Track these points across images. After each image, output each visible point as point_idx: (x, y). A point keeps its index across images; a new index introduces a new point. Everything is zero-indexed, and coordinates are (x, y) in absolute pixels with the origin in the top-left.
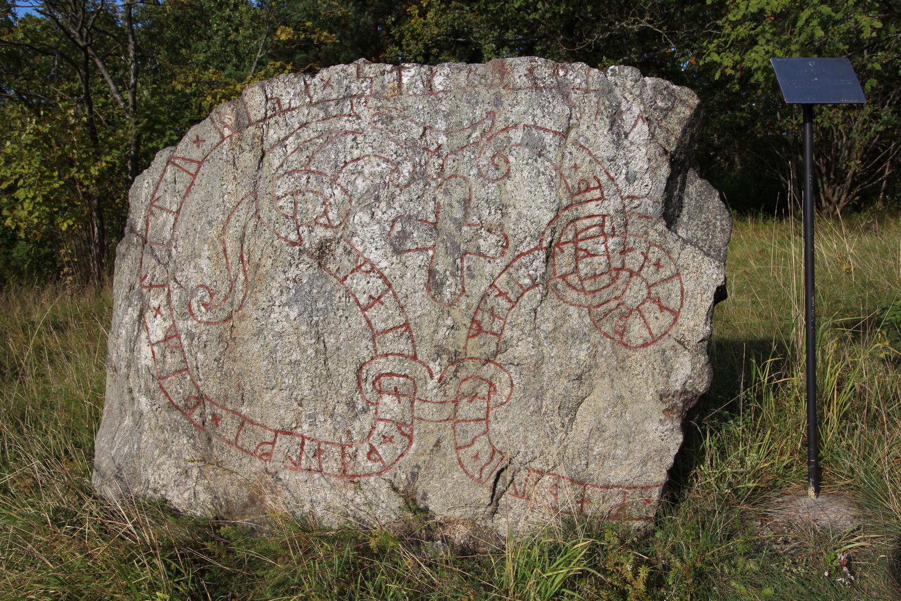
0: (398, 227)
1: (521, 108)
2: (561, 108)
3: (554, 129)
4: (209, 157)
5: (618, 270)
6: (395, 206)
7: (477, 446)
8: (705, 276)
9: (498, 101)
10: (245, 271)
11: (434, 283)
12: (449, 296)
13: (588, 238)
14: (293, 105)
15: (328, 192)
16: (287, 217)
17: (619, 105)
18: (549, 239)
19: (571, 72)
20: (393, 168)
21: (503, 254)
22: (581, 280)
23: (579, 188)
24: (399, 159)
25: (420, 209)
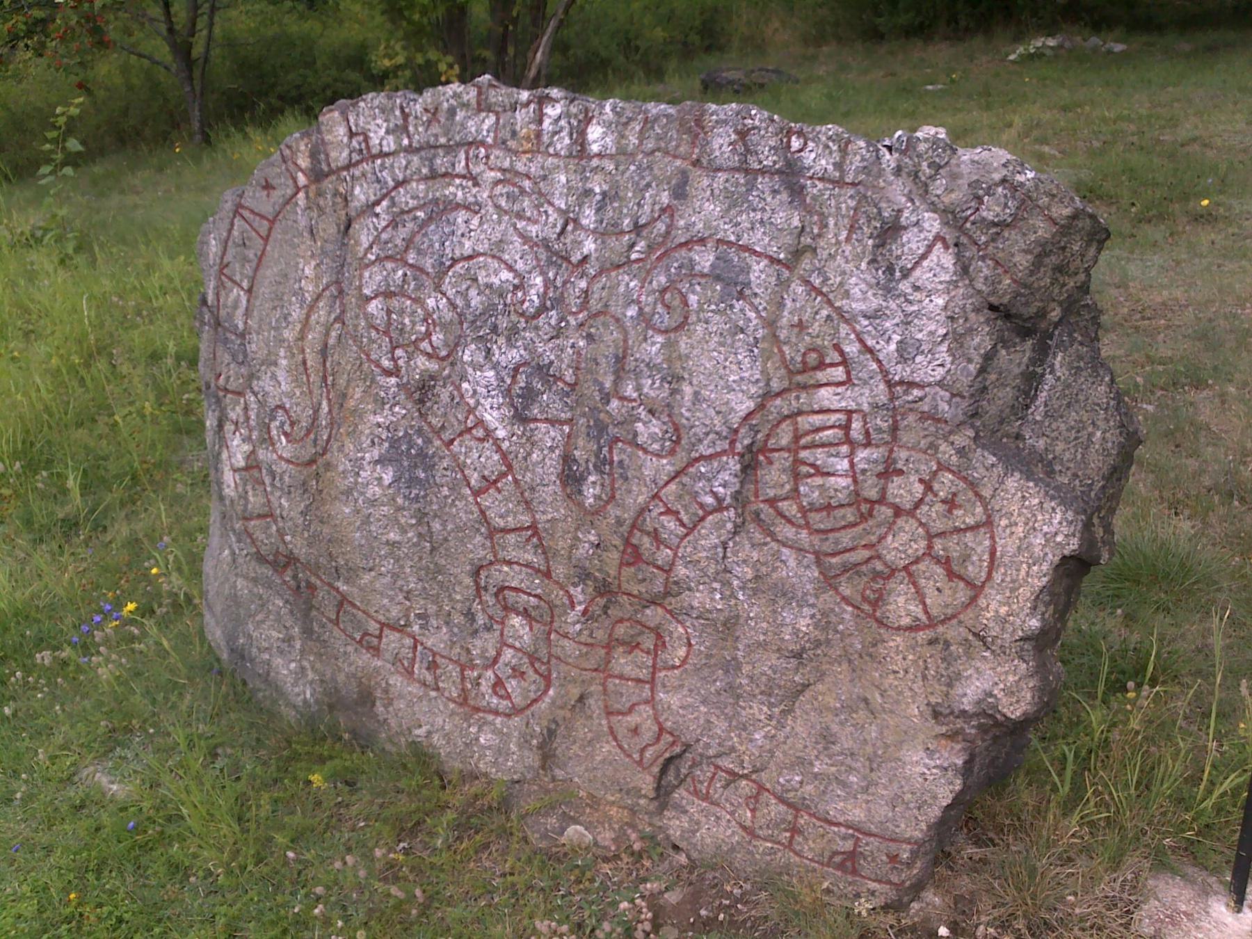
0: (522, 380)
11: (571, 478)
14: (385, 149)
21: (672, 452)
22: (802, 509)
23: (804, 362)
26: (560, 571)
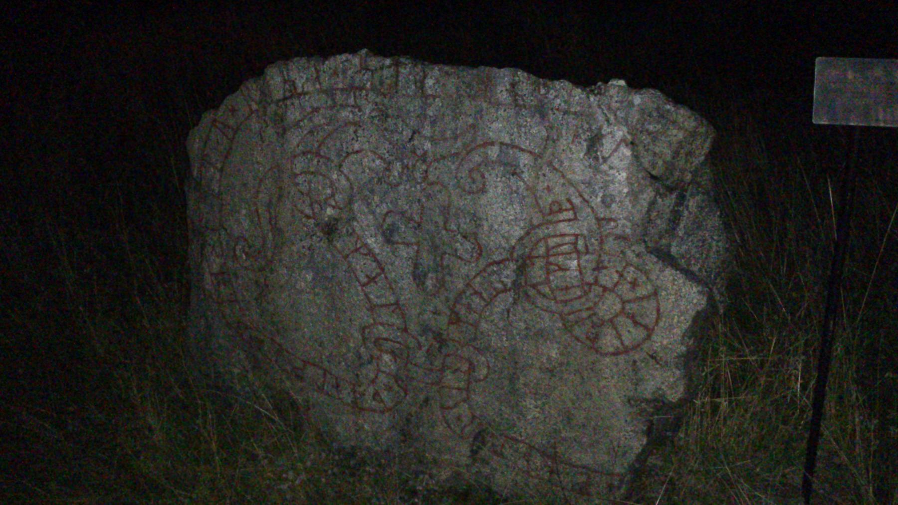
0: (389, 220)
1: (497, 125)
2: (538, 131)
5: (590, 285)
11: (419, 277)
13: (559, 254)
16: (303, 194)
17: (600, 128)
19: (552, 91)
21: (477, 259)
22: (552, 291)
23: (551, 209)
24: (391, 158)
26: (412, 327)
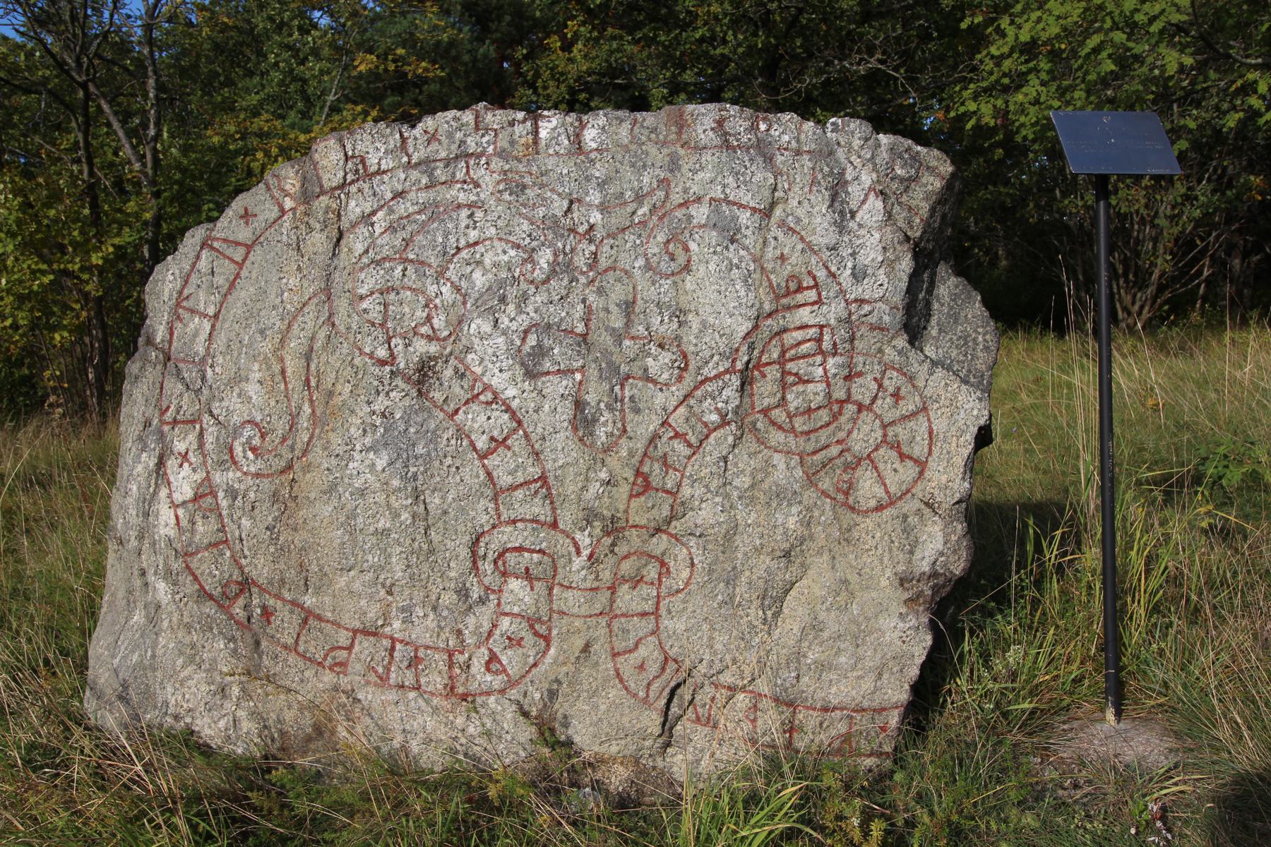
0: (532, 340)
1: (706, 175)
2: (761, 176)
3: (752, 204)
4: (262, 239)
5: (841, 403)
6: (528, 310)
7: (642, 652)
8: (962, 411)
9: (674, 165)
10: (311, 401)
11: (582, 420)
12: (604, 438)
13: (799, 358)
14: (383, 167)
15: (432, 289)
16: (373, 324)
17: (842, 173)
18: (746, 358)
20: (525, 256)
21: (680, 379)
22: (790, 416)
24: (534, 244)
25: (563, 314)
26: (566, 520)
